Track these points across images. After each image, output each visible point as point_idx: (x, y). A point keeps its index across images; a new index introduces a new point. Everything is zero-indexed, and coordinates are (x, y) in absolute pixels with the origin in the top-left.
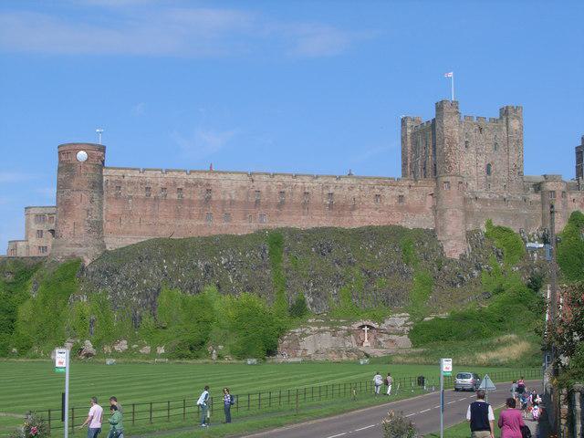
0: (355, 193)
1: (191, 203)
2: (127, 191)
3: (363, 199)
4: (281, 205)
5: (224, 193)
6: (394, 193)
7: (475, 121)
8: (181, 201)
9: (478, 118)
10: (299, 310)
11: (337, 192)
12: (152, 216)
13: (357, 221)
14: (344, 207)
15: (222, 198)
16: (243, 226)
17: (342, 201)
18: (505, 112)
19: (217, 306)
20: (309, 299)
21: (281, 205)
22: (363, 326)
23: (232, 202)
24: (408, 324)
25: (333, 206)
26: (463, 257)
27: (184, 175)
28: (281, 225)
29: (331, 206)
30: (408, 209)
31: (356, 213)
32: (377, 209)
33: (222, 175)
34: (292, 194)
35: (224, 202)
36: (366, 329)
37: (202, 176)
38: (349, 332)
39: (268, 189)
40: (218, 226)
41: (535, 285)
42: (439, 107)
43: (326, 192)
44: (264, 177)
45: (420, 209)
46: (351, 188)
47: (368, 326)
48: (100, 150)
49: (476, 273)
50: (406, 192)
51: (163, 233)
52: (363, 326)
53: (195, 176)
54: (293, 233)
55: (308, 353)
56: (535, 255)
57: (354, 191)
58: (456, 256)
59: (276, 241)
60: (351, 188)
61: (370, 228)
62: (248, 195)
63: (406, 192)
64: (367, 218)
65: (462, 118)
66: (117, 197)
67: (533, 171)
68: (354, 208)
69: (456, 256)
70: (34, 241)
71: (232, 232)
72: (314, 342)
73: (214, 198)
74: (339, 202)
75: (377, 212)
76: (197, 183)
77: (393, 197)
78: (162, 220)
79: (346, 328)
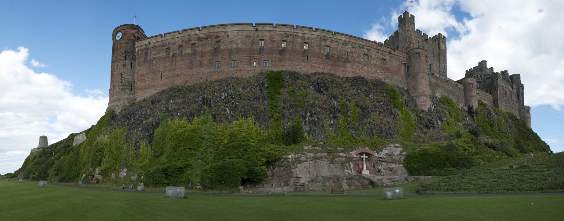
0: (348, 48)
3: (355, 54)
5: (231, 42)
10: (293, 138)
14: (339, 58)
15: (229, 47)
20: (306, 128)
22: (362, 154)
23: (238, 50)
24: (404, 153)
27: (197, 32)
31: (349, 65)
33: (229, 27)
34: (293, 43)
35: (230, 51)
36: (364, 157)
37: (212, 30)
38: (349, 159)
40: (223, 70)
44: (268, 28)
52: (362, 154)
53: (206, 31)
55: (302, 181)
57: (347, 47)
59: (276, 79)
60: (345, 44)
63: (387, 57)
68: (347, 61)
72: (308, 168)
73: (222, 47)
79: (344, 155)
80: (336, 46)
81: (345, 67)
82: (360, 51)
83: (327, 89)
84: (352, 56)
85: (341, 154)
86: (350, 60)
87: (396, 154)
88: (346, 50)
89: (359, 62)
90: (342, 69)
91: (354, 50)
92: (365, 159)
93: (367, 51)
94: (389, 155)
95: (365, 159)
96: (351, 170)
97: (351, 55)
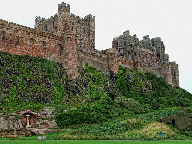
0: (19, 34)
3: (23, 39)
6: (41, 39)
7: (76, 17)
9: (77, 17)
11: (8, 31)
13: (18, 51)
17: (11, 38)
22: (26, 114)
26: (77, 79)
30: (48, 49)
31: (19, 46)
32: (31, 46)
36: (28, 115)
45: (54, 52)
46: (17, 31)
47: (30, 114)
49: (84, 88)
50: (47, 40)
52: (26, 114)
56: (108, 82)
57: (18, 33)
58: (74, 78)
61: (27, 56)
64: (25, 50)
65: (71, 15)
68: (18, 43)
69: (74, 78)
74: (9, 38)
75: (31, 48)
77: (40, 41)
79: (15, 114)
80: (10, 32)
81: (16, 48)
82: (27, 36)
84: (22, 40)
85: (13, 114)
86: (20, 42)
87: (49, 113)
88: (17, 36)
89: (26, 44)
90: (14, 49)
91: (23, 36)
92: (28, 117)
93: (32, 36)
94: (45, 114)
95: (28, 117)
96: (19, 124)
97: (21, 39)
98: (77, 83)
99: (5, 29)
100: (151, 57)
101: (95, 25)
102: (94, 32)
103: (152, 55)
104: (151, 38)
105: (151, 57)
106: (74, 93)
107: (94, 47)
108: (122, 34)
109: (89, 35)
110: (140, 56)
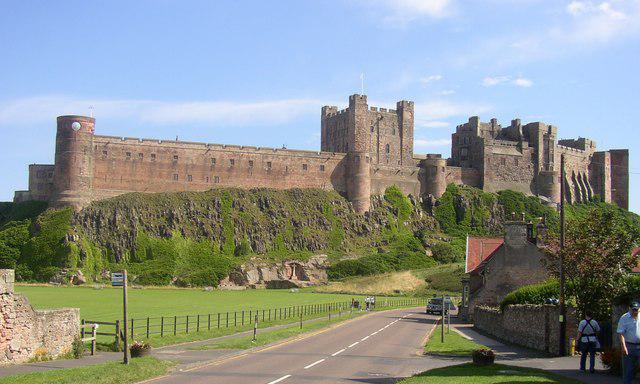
0: (288, 163)
1: (161, 165)
2: (112, 155)
4: (230, 170)
5: (188, 158)
8: (154, 164)
12: (131, 175)
16: (200, 186)
17: (278, 168)
18: (401, 108)
19: (178, 246)
21: (230, 170)
23: (193, 166)
25: (270, 171)
26: (367, 214)
28: (231, 185)
29: (269, 172)
31: (287, 178)
39: (222, 157)
40: (183, 185)
41: (419, 235)
42: (353, 100)
43: (265, 161)
48: (91, 121)
49: (377, 226)
51: (139, 188)
54: (241, 194)
62: (205, 161)
66: (103, 159)
67: (422, 147)
68: (286, 174)
69: (363, 213)
70: (35, 191)
71: (192, 189)
76: (167, 150)
78: (138, 178)
83: (267, 206)
98: (367, 220)
99: (270, 160)
100: (516, 160)
101: (412, 116)
102: (411, 129)
103: (516, 159)
104: (524, 123)
105: (516, 160)
106: (359, 234)
107: (411, 152)
108: (467, 121)
109: (401, 136)
110: (489, 164)
